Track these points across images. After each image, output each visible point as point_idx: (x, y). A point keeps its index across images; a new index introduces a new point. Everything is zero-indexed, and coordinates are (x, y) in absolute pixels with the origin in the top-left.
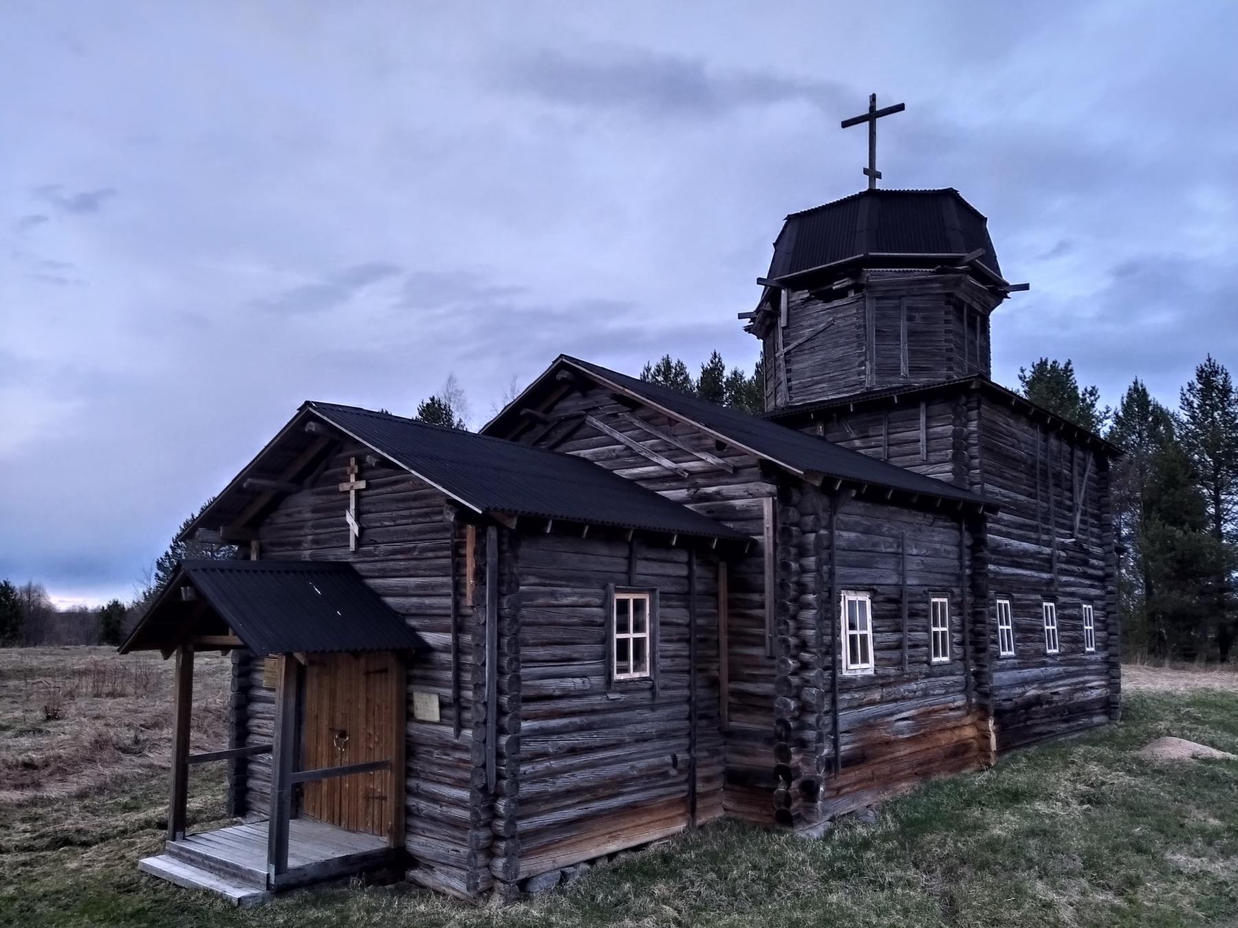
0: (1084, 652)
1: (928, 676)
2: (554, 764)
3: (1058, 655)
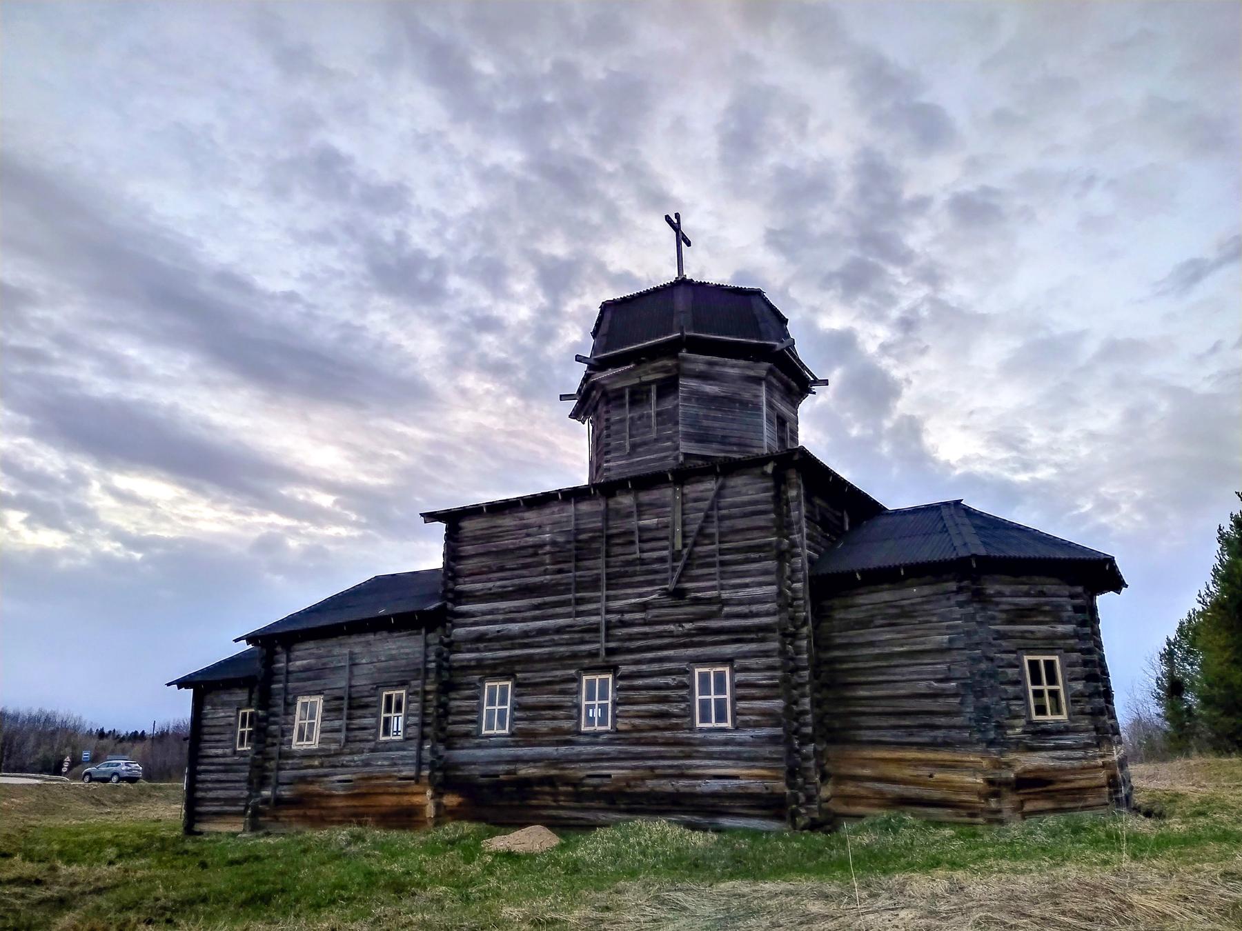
0: (692, 729)
1: (373, 750)
2: (210, 785)
3: (607, 732)
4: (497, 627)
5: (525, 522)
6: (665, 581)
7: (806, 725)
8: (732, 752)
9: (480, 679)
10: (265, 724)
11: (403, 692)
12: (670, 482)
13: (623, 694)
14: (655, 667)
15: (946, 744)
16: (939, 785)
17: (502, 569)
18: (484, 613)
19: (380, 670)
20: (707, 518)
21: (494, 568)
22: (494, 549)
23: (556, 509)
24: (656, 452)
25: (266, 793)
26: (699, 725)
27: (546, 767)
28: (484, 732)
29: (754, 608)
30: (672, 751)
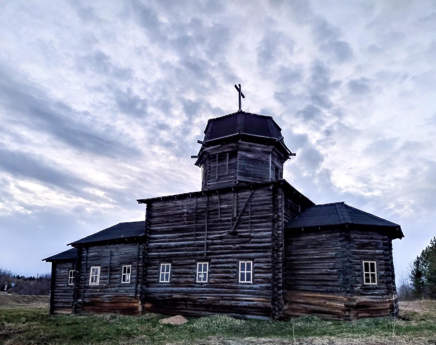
0: (237, 283)
1: (119, 287)
2: (59, 297)
3: (206, 283)
4: (166, 244)
5: (177, 204)
6: (229, 229)
7: (280, 283)
8: (252, 292)
9: (159, 262)
10: (79, 276)
11: (130, 266)
12: (233, 191)
13: (212, 270)
14: (224, 260)
15: (332, 292)
16: (328, 306)
17: (168, 222)
18: (161, 238)
19: (121, 258)
20: (246, 206)
21: (165, 222)
22: (165, 214)
23: (189, 200)
24: (228, 179)
25: (80, 300)
26: (240, 282)
27: (183, 295)
28: (160, 281)
29: (263, 240)
30: (230, 291)
